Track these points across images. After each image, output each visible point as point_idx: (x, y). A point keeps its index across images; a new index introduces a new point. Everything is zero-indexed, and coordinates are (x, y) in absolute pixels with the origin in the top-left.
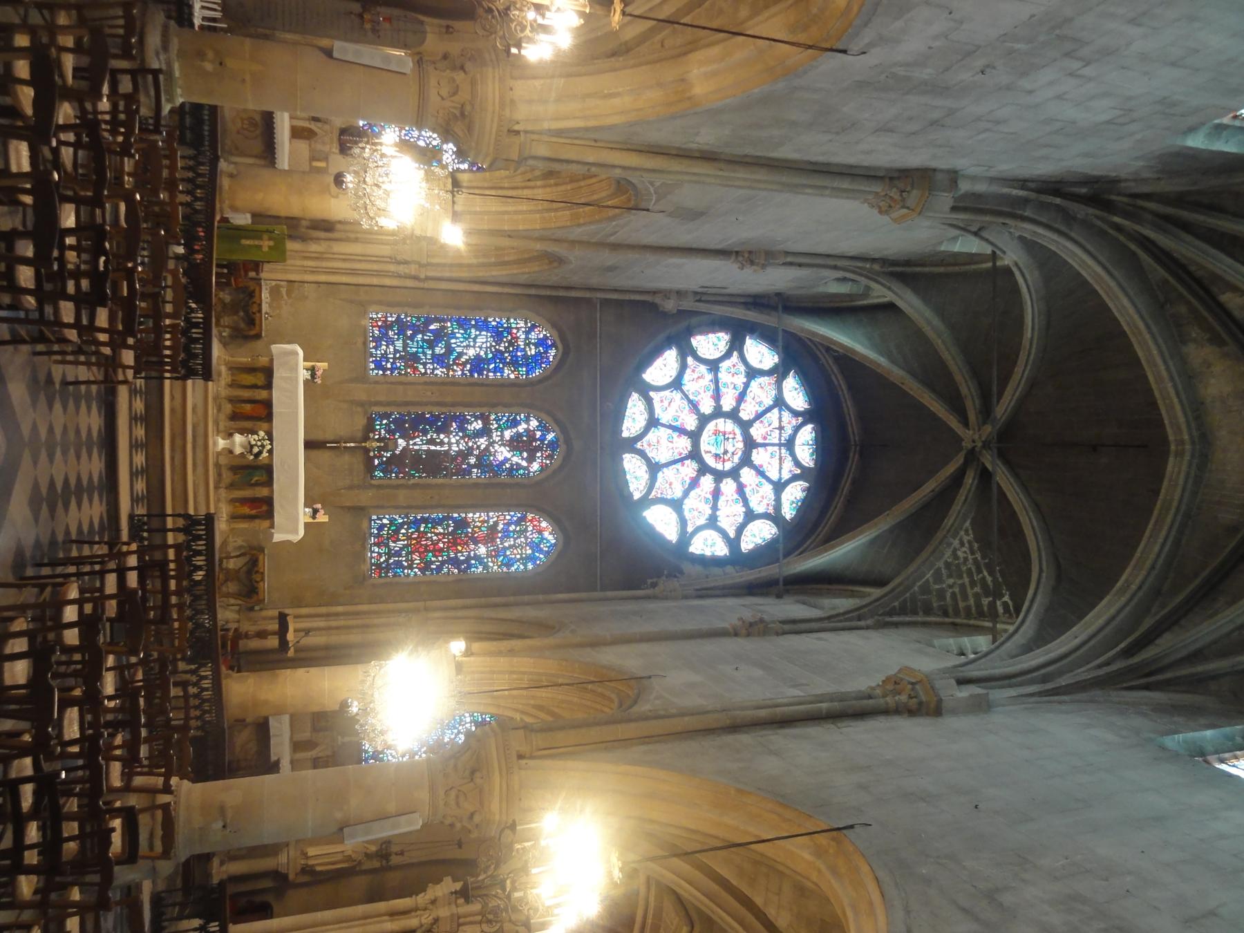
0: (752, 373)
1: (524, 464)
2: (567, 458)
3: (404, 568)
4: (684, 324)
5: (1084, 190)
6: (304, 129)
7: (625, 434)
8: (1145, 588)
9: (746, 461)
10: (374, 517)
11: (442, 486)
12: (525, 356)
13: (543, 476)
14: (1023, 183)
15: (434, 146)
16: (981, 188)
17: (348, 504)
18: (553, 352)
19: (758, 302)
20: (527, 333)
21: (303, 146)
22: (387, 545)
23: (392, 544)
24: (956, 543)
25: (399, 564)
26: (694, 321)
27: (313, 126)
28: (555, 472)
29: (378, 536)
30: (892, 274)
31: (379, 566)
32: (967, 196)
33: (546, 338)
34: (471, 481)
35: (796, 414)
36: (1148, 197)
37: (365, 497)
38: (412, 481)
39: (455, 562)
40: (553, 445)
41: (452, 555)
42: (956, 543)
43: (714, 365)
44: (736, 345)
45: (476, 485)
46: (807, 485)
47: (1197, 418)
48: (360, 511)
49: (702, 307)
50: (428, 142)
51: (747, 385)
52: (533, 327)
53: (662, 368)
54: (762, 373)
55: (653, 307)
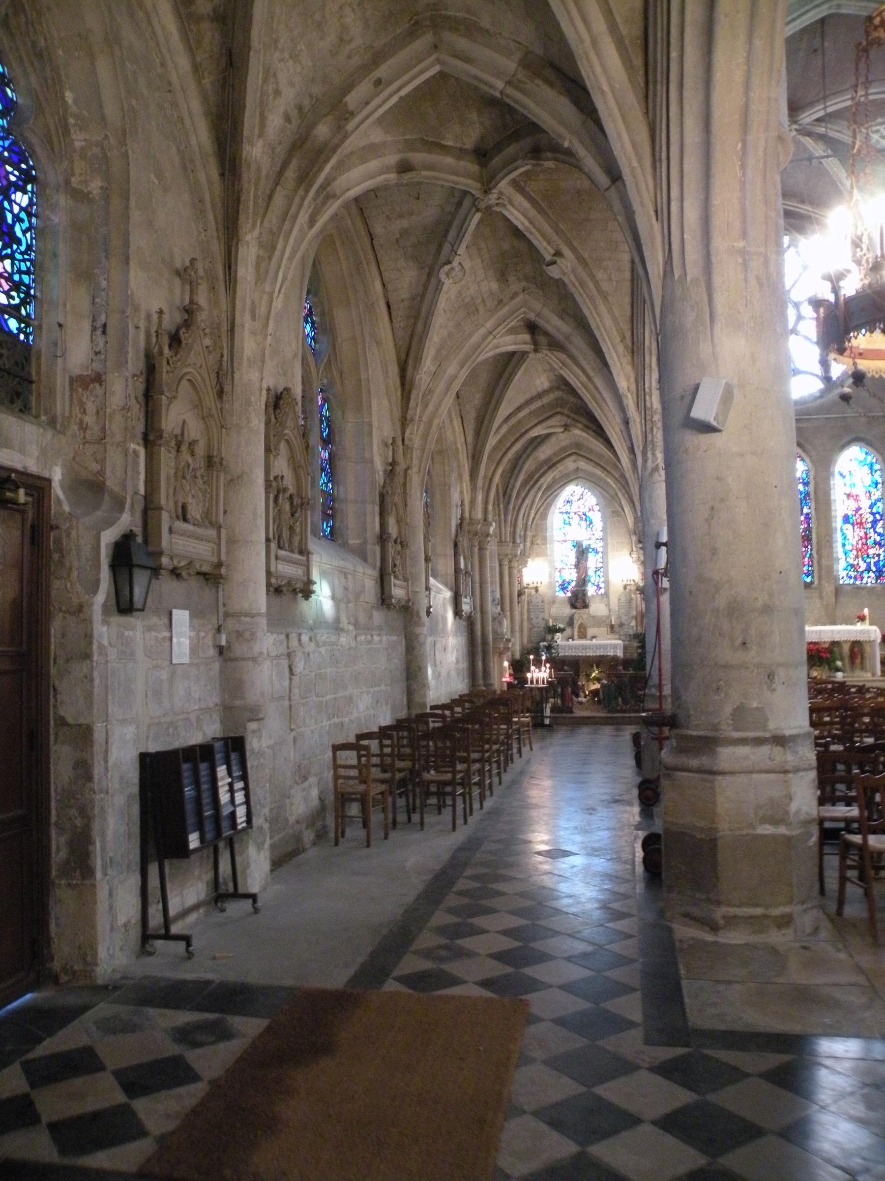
3: (879, 561)
6: (579, 631)
10: (841, 582)
11: (817, 534)
13: (807, 460)
17: (834, 599)
21: (591, 632)
22: (862, 572)
23: (861, 570)
25: (876, 564)
27: (576, 626)
29: (855, 578)
31: (877, 578)
34: (813, 513)
37: (829, 589)
38: (815, 555)
39: (874, 523)
41: (869, 525)
45: (816, 509)
48: (839, 590)
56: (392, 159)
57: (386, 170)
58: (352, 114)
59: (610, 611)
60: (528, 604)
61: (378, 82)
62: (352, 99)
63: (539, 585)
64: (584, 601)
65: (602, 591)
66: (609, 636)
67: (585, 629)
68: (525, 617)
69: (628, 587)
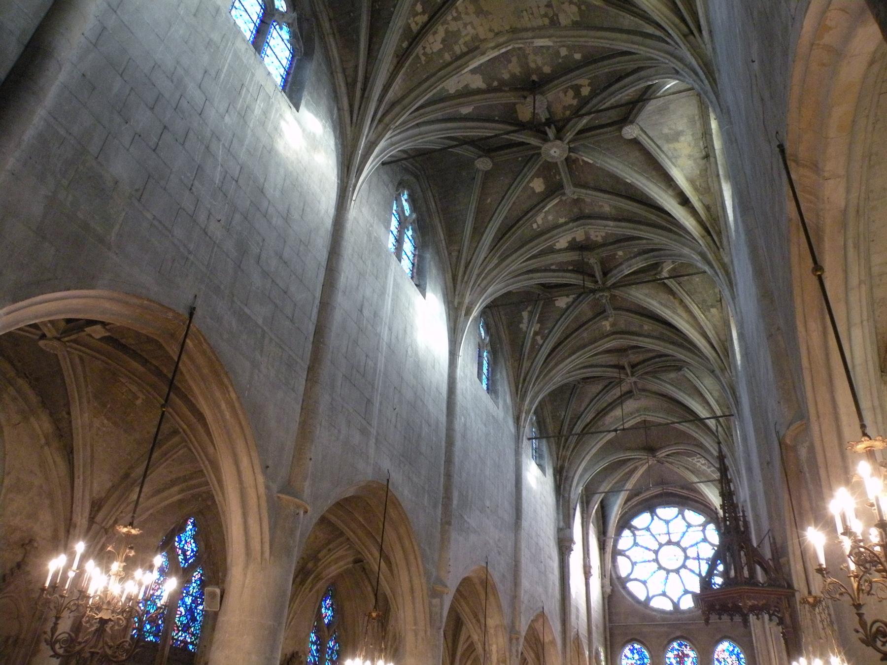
0: (636, 544)
1: (690, 659)
2: (686, 639)
4: (616, 582)
5: (558, 477)
7: (672, 609)
8: (696, 430)
9: (678, 544)
12: (639, 660)
14: (558, 501)
16: (561, 517)
18: (636, 646)
19: (602, 547)
20: (628, 658)
24: (699, 464)
26: (614, 576)
28: (693, 644)
30: (587, 507)
32: (564, 522)
33: (630, 649)
35: (653, 519)
36: (557, 454)
40: (680, 645)
42: (699, 464)
43: (634, 564)
44: (622, 553)
46: (686, 511)
47: (631, 414)
49: (608, 575)
51: (642, 547)
52: (626, 656)
53: (637, 590)
54: (635, 540)
55: (610, 597)
56: (351, 559)
57: (348, 563)
58: (320, 560)
61: (329, 550)
62: (320, 555)
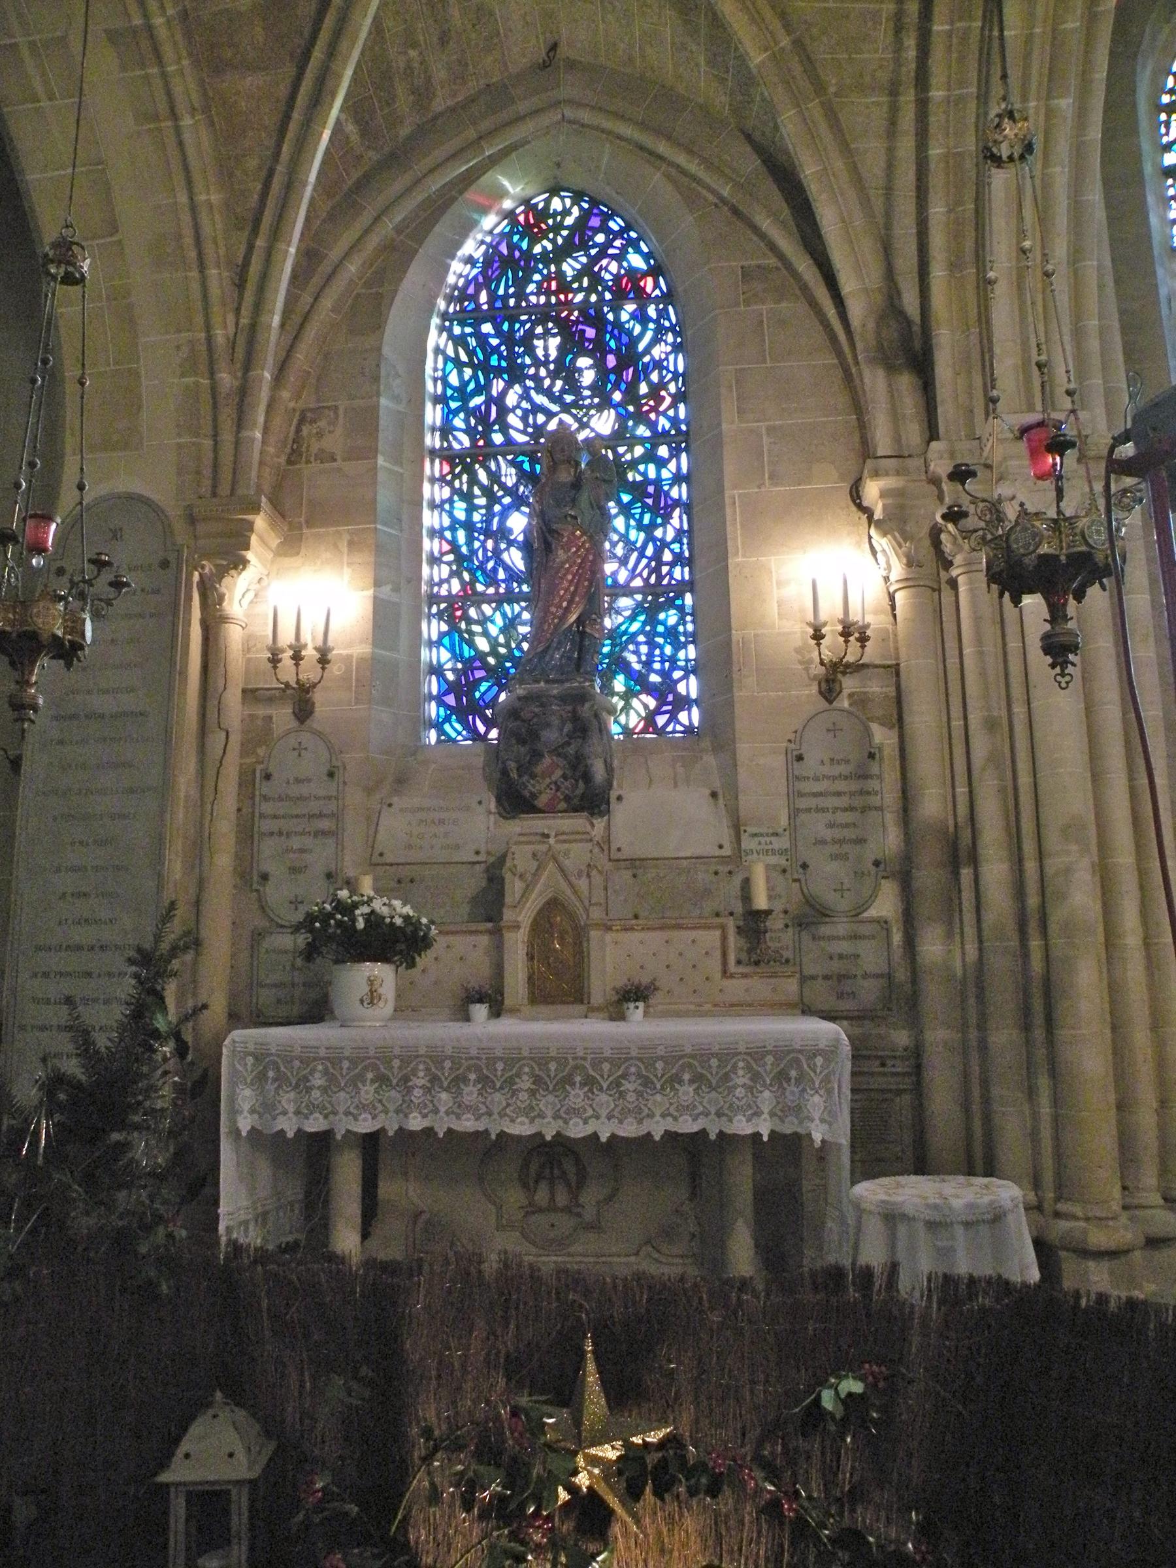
15: (522, 475)
50: (507, 500)
59: (737, 828)
60: (247, 782)
63: (309, 671)
64: (579, 768)
65: (692, 717)
66: (736, 988)
67: (579, 936)
68: (223, 861)
69: (849, 684)
